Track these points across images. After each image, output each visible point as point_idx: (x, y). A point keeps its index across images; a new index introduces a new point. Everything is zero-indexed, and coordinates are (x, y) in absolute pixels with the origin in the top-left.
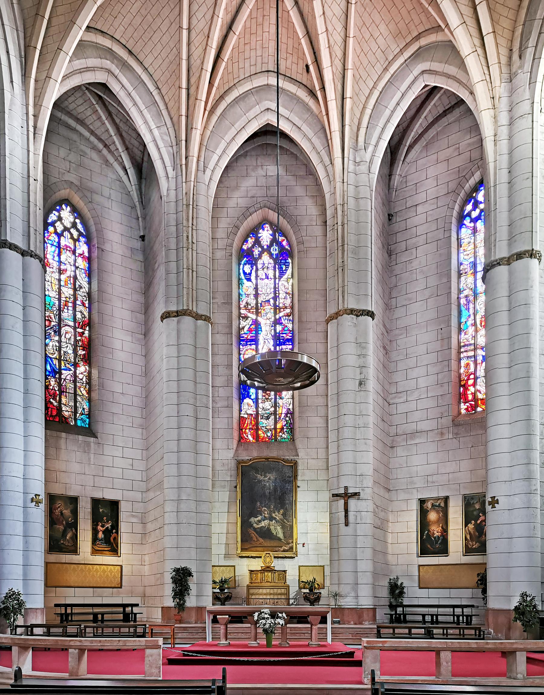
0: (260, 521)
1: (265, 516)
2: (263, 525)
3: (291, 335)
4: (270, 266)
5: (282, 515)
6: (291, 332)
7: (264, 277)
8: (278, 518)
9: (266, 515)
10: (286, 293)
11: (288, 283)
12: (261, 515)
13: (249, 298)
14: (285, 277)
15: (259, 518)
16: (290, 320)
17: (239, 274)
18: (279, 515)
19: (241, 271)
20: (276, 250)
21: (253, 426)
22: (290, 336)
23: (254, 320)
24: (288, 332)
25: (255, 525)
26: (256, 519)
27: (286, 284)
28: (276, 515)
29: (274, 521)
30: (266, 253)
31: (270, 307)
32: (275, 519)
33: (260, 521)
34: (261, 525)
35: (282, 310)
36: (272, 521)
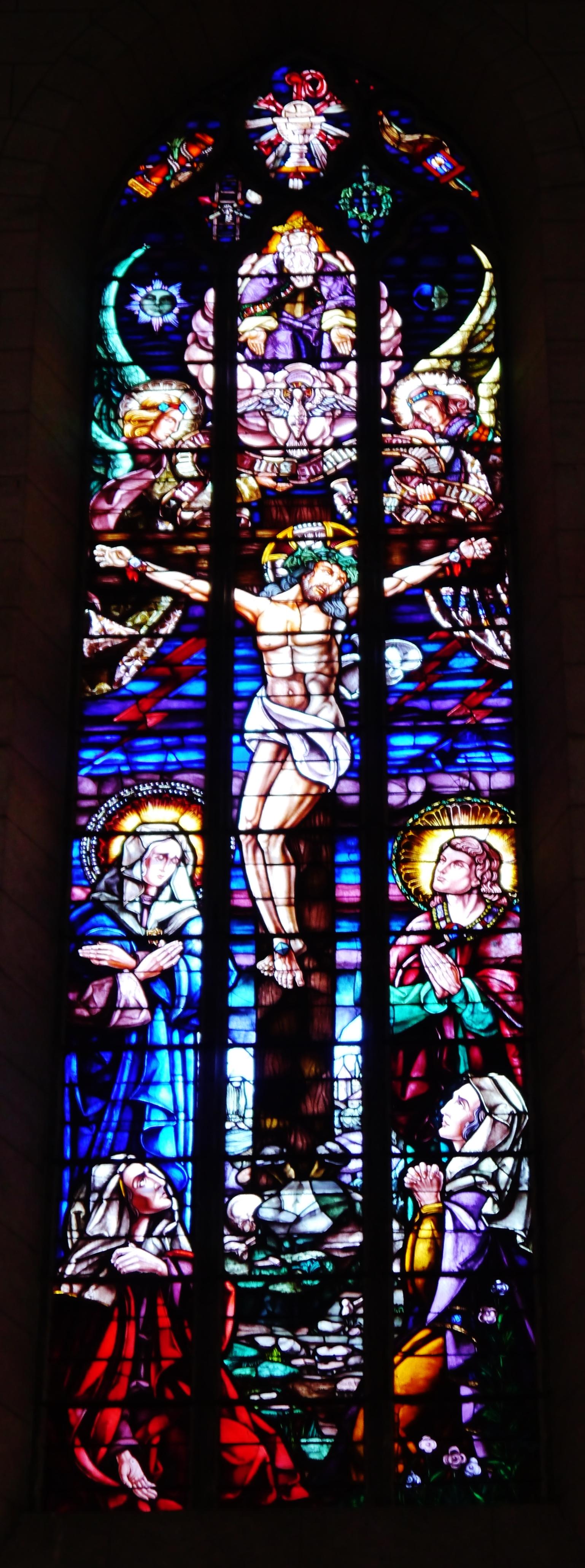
3: (504, 702)
4: (327, 285)
6: (509, 686)
7: (285, 352)
10: (458, 442)
11: (472, 385)
13: (163, 474)
14: (453, 344)
16: (494, 608)
17: (101, 334)
19: (109, 318)
20: (375, 202)
21: (168, 1378)
22: (496, 712)
23: (198, 611)
24: (480, 683)
27: (456, 390)
30: (297, 220)
31: (330, 528)
35: (427, 545)
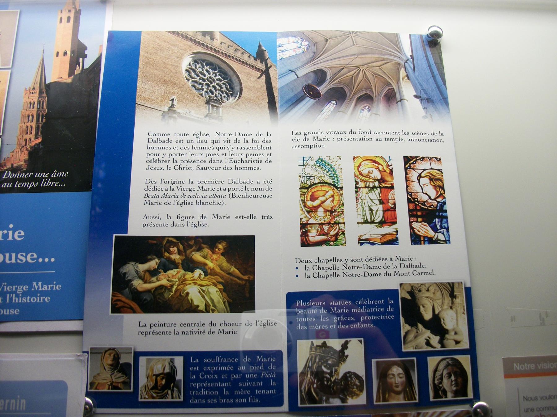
0: (153, 273)
1: (169, 259)
2: (164, 282)
5: (223, 254)
8: (210, 264)
9: (176, 257)
12: (159, 255)
15: (153, 264)
18: (215, 256)
25: (138, 284)
26: (142, 267)
28: (205, 257)
29: (198, 272)
32: (202, 266)
33: (153, 273)
34: (158, 284)
36: (192, 271)
